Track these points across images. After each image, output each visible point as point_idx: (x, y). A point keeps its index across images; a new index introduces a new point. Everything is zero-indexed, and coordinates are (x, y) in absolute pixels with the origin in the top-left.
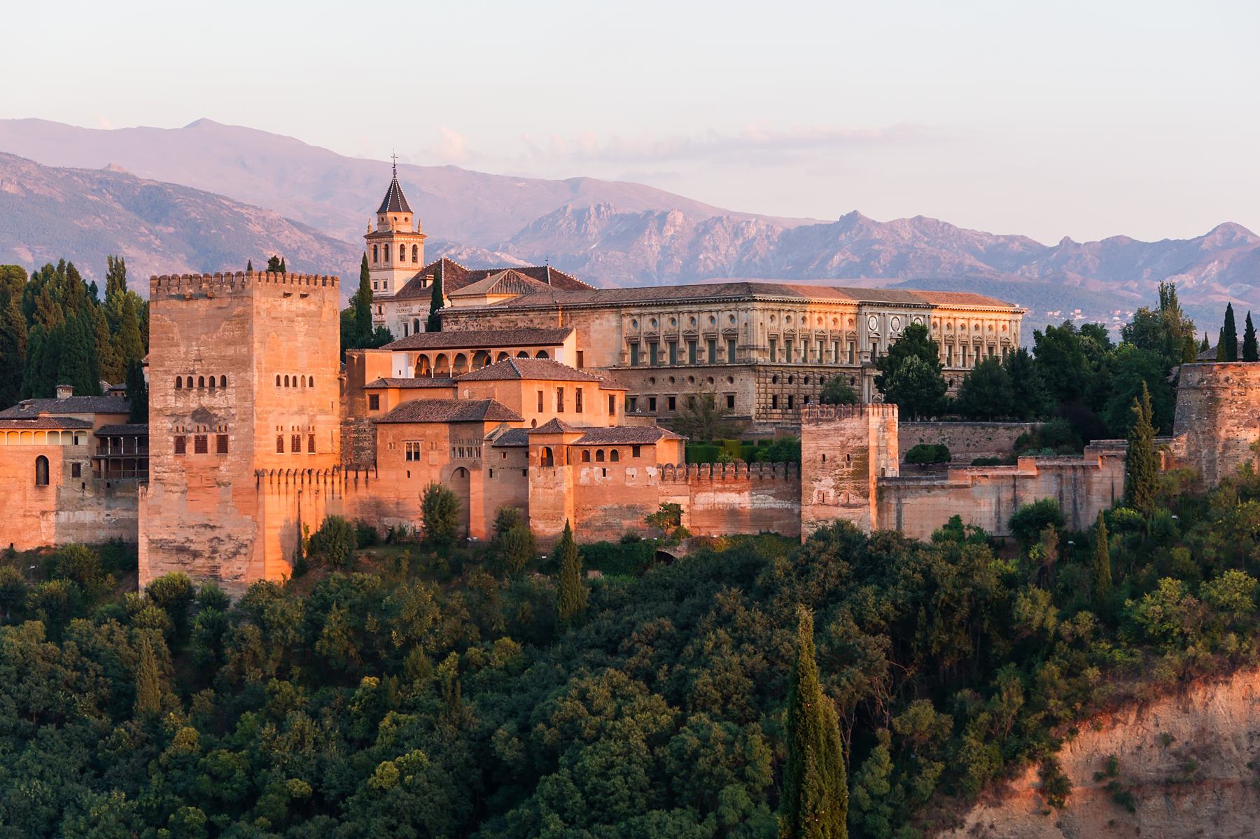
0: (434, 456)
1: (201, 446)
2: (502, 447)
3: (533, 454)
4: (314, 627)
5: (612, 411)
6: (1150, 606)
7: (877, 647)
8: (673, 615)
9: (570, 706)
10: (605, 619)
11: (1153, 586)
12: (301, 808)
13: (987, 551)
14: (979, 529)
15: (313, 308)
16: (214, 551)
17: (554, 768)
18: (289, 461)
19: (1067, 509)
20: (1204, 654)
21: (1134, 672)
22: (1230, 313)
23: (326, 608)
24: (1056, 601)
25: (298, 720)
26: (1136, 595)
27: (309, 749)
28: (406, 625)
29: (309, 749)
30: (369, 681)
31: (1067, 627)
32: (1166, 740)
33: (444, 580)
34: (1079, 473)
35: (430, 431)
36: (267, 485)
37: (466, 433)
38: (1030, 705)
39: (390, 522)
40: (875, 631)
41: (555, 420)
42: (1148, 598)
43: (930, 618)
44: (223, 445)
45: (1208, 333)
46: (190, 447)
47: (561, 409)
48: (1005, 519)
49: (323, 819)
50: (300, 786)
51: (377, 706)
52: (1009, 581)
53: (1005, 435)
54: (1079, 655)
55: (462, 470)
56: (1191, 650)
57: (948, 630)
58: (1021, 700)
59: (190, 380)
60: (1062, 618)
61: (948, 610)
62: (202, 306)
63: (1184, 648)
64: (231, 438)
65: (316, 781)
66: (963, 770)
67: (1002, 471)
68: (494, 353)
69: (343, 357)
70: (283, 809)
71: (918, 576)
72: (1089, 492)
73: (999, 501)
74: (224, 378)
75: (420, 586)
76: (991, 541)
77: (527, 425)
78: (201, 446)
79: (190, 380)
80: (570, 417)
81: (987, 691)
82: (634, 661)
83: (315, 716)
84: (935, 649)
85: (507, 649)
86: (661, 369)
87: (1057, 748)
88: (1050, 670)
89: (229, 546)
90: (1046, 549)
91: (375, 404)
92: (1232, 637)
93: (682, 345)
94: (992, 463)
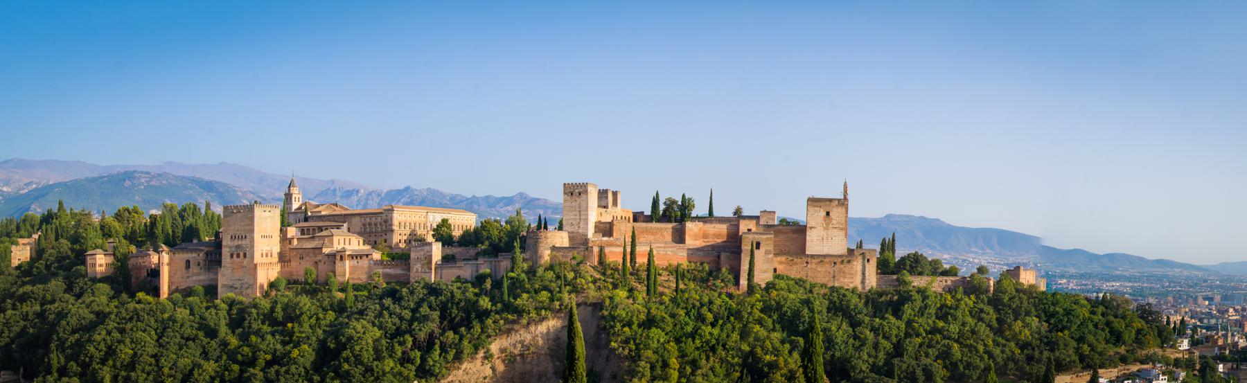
0: (308, 258)
1: (238, 256)
2: (328, 255)
3: (337, 257)
4: (273, 309)
5: (359, 244)
6: (519, 301)
7: (436, 315)
8: (379, 304)
9: (350, 331)
10: (360, 306)
11: (519, 296)
12: (269, 364)
13: (469, 285)
14: (466, 280)
15: (272, 215)
16: (242, 287)
17: (346, 349)
18: (265, 260)
19: (493, 274)
20: (535, 316)
21: (514, 322)
22: (540, 217)
23: (276, 302)
24: (491, 300)
25: (269, 337)
26: (515, 299)
27: (271, 346)
28: (301, 308)
29: (271, 346)
30: (290, 325)
31: (494, 308)
32: (522, 342)
33: (311, 294)
34: (497, 263)
35: (307, 251)
36: (258, 268)
37: (317, 251)
38: (483, 331)
39: (294, 277)
40: (435, 310)
41: (344, 248)
42: (518, 299)
43: (452, 305)
44: (245, 256)
45: (534, 225)
46: (235, 256)
47: (345, 244)
48: (474, 276)
49: (276, 367)
50: (269, 357)
51: (291, 334)
52: (476, 295)
53: (472, 251)
54: (498, 317)
55: (316, 262)
56: (531, 315)
57: (458, 309)
58: (480, 330)
59: (235, 237)
60: (492, 305)
61: (458, 304)
62: (239, 215)
63: (529, 314)
64: (247, 253)
65: (274, 355)
66: (462, 352)
67: (473, 262)
68: (324, 228)
69: (281, 230)
70: (264, 364)
71: (449, 294)
72: (500, 268)
73: (472, 271)
74: (245, 237)
75: (304, 296)
76: (470, 282)
77: (335, 249)
78: (238, 256)
79: (235, 237)
80: (347, 247)
81: (469, 327)
82: (368, 317)
83: (273, 335)
84: (453, 315)
85: (331, 315)
86: (372, 232)
87: (490, 344)
88: (489, 321)
89: (246, 286)
90: (488, 284)
91: (290, 244)
92: (543, 311)
93: (379, 226)
94: (469, 260)
